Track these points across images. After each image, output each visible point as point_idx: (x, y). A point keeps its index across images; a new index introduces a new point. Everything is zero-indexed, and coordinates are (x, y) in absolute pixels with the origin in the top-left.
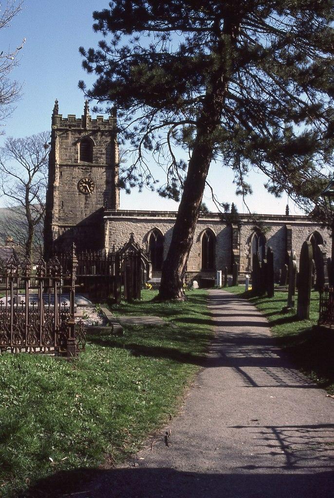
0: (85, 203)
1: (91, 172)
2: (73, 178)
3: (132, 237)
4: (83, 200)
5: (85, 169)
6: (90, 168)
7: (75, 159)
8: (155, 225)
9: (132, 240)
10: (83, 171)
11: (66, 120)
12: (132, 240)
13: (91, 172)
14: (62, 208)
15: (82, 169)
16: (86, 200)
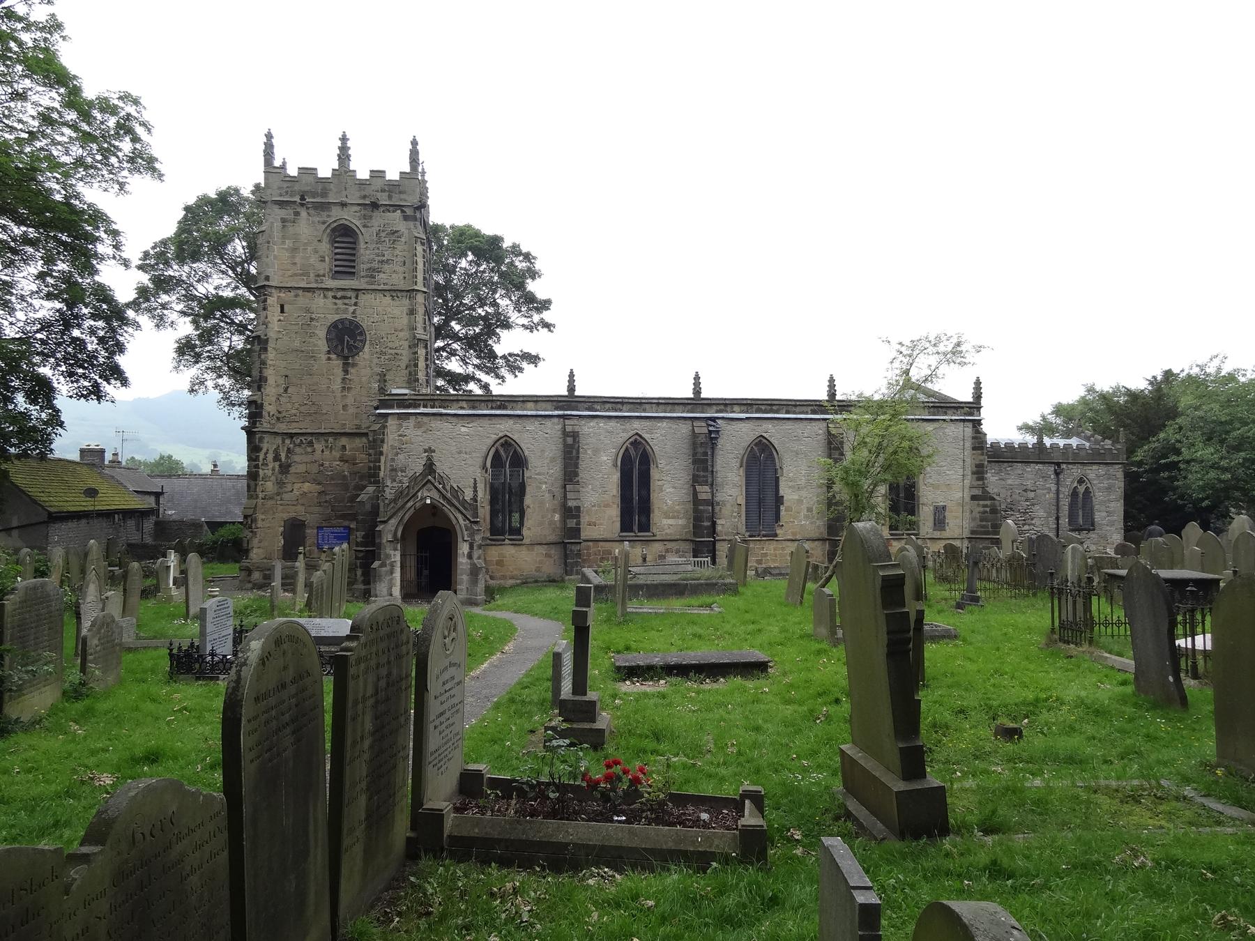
0: (344, 379)
1: (356, 304)
2: (312, 319)
3: (429, 459)
4: (339, 372)
5: (344, 297)
6: (352, 294)
7: (318, 276)
8: (504, 427)
9: (430, 467)
10: (336, 304)
11: (293, 180)
12: (430, 467)
13: (356, 304)
14: (286, 390)
15: (335, 297)
16: (346, 372)
